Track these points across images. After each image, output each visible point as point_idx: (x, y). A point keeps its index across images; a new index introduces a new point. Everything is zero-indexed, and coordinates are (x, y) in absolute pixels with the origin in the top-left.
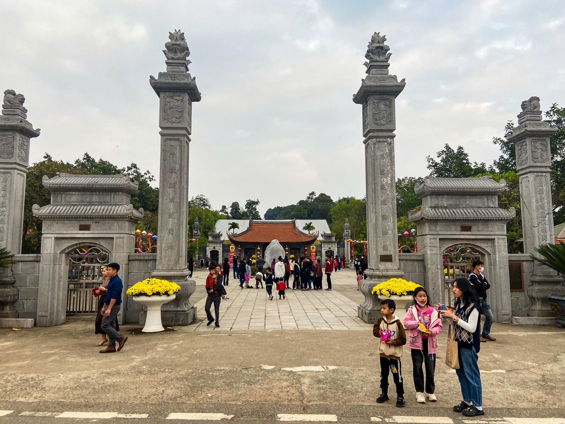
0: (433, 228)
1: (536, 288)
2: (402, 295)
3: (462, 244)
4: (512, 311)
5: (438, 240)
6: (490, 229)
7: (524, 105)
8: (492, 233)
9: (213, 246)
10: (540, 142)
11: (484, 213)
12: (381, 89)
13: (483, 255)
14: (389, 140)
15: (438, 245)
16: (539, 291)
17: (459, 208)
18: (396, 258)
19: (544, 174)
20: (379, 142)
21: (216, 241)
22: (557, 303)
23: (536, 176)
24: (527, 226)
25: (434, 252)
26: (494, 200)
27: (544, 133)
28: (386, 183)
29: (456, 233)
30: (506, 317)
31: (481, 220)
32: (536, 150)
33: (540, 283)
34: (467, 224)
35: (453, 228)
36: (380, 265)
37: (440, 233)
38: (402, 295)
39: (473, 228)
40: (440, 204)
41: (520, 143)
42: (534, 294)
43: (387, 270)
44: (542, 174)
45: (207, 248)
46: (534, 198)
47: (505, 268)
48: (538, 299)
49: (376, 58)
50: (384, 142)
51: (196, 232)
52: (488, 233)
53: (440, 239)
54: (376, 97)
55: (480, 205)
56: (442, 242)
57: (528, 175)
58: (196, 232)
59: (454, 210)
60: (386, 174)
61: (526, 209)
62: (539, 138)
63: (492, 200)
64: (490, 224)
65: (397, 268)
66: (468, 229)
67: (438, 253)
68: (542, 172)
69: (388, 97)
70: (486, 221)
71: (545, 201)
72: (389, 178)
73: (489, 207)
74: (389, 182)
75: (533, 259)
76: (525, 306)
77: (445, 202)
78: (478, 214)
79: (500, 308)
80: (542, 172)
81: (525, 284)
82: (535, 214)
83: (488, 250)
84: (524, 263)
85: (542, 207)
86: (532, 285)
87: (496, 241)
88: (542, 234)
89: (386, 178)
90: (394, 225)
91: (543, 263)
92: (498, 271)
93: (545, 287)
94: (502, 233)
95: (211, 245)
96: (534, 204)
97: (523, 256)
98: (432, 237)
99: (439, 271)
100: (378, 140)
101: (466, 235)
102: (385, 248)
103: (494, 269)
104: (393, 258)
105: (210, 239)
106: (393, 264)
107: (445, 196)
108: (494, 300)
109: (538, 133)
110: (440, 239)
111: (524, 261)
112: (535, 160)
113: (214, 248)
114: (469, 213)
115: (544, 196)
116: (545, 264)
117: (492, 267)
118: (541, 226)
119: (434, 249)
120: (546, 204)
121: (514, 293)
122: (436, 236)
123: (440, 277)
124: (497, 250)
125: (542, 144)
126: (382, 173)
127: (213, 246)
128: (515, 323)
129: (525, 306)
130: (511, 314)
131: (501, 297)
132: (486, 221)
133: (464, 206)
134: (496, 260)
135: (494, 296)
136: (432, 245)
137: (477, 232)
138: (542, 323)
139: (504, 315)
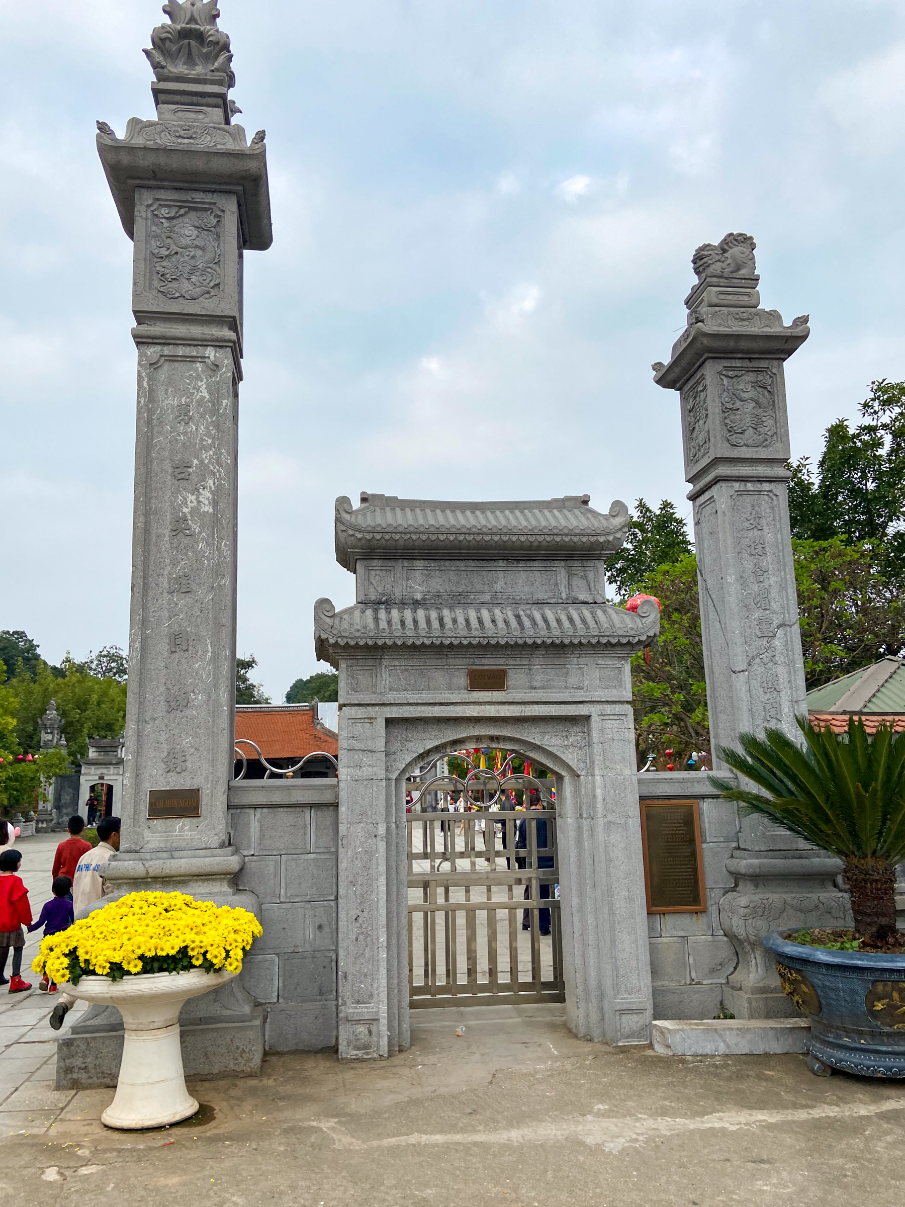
0: (363, 678)
1: (743, 901)
2: (117, 971)
3: (478, 739)
4: (656, 992)
6: (572, 680)
7: (701, 260)
8: (579, 696)
9: (99, 772)
10: (751, 377)
11: (553, 622)
12: (175, 163)
14: (210, 352)
15: (381, 743)
16: (754, 911)
17: (466, 605)
18: (214, 803)
19: (766, 486)
20: (173, 359)
21: (107, 759)
22: (799, 971)
23: (740, 493)
24: (716, 669)
25: (367, 772)
26: (591, 575)
27: (761, 345)
28: (195, 511)
29: (447, 692)
30: (632, 1022)
31: (535, 646)
32: (738, 404)
33: (758, 879)
34: (489, 663)
35: (440, 677)
36: (147, 835)
37: (390, 697)
38: (117, 971)
39: (516, 678)
40: (398, 593)
41: (693, 388)
42: (738, 926)
43: (172, 852)
44: (758, 486)
45: (83, 779)
46: (731, 570)
47: (626, 827)
48: (753, 945)
49: (180, 68)
50: (193, 359)
51: (50, 737)
53: (389, 722)
54: (162, 195)
55: (541, 596)
56: (399, 733)
57: (714, 491)
58: (50, 737)
59: (446, 612)
60: (194, 477)
61: (712, 615)
62: (746, 363)
63: (585, 577)
64: (573, 662)
65: (215, 841)
66: (493, 680)
67: (382, 774)
68: (760, 480)
69: (208, 198)
70: (558, 650)
71: (773, 580)
72: (207, 494)
73: (575, 602)
74: (207, 508)
75: (728, 793)
76: (713, 971)
77: (417, 581)
78: (527, 623)
79: (609, 992)
80: (760, 480)
81: (709, 883)
82: (735, 626)
83: (570, 757)
84: (706, 806)
85: (762, 601)
86: (733, 889)
87: (595, 722)
88: (764, 698)
89: (195, 491)
90: (217, 668)
91: (756, 804)
92: (601, 836)
93: (775, 897)
94: (613, 695)
95: (93, 770)
96: (732, 590)
97: (692, 781)
98: (360, 712)
99: (382, 846)
100: (167, 350)
101: (487, 704)
102: (174, 761)
103: (592, 829)
104: (204, 800)
105: (92, 753)
106: (202, 822)
107: (419, 564)
108: (592, 952)
109: (743, 345)
110: (389, 722)
111: (703, 797)
112: (734, 439)
113: (101, 778)
114: (498, 624)
115: (768, 561)
116: (757, 809)
117: (585, 823)
118: (757, 668)
119: (366, 759)
120: (774, 593)
121: (670, 920)
123: (383, 869)
124: (598, 758)
125: (756, 384)
126: (181, 472)
127: (99, 772)
128: (660, 1049)
129: (713, 971)
130: (649, 1006)
131: (613, 941)
132: (558, 650)
133: (487, 597)
134: (595, 796)
135: (591, 938)
136: (357, 745)
137: (529, 690)
138: (760, 1049)
139: (622, 1012)
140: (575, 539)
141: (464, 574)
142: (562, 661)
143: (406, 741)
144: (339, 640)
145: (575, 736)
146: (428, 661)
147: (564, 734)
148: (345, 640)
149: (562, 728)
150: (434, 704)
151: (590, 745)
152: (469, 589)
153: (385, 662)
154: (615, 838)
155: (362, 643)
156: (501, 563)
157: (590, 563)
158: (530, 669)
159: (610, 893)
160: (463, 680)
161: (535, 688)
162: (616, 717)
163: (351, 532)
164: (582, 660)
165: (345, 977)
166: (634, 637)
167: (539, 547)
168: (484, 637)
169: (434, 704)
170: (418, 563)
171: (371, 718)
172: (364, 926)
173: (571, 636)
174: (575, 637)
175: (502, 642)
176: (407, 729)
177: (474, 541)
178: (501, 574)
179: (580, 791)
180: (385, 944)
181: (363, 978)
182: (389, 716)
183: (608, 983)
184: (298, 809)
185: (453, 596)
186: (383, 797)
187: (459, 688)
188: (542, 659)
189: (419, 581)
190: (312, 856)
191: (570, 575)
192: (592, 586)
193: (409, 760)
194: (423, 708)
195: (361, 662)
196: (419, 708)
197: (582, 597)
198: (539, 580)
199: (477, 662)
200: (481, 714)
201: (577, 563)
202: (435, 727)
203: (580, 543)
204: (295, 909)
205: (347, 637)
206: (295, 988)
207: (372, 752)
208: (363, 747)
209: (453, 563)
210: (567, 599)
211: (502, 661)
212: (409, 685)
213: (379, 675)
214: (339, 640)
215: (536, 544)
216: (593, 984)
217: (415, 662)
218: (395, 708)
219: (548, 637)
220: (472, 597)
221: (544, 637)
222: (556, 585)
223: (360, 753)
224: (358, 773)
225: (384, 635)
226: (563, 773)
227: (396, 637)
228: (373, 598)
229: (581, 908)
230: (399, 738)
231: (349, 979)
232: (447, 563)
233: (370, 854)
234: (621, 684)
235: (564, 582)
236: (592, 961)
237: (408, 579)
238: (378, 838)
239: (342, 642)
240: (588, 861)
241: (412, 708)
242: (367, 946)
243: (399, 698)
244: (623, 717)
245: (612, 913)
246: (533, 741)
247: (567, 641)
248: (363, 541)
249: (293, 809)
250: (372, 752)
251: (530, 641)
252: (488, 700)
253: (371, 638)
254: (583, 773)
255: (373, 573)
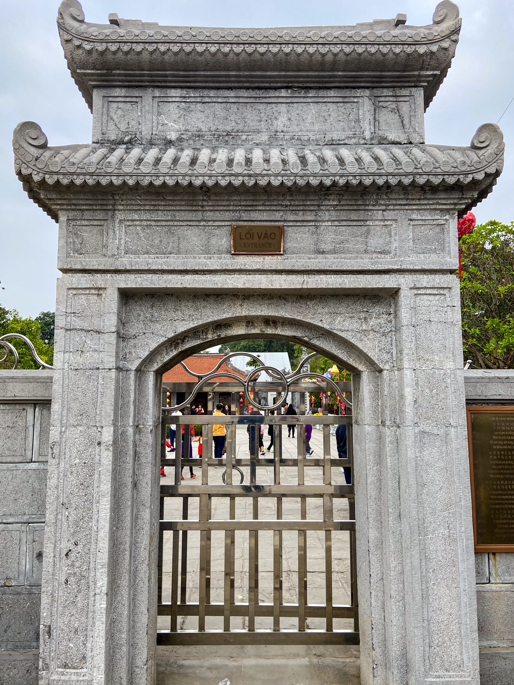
3: (249, 321)
5: (112, 299)
6: (374, 242)
13: (357, 374)
15: (111, 322)
25: (90, 359)
26: (405, 108)
29: (201, 253)
34: (262, 217)
35: (193, 237)
39: (297, 238)
40: (146, 131)
47: (446, 439)
52: (365, 263)
53: (127, 296)
56: (141, 311)
66: (264, 241)
67: (111, 361)
73: (383, 141)
83: (369, 346)
87: (405, 298)
92: (410, 452)
94: (432, 261)
98: (84, 281)
99: (106, 458)
101: (257, 272)
103: (397, 441)
108: (393, 606)
110: (127, 296)
117: (388, 433)
119: (90, 342)
122: (100, 280)
124: (408, 346)
131: (425, 597)
134: (402, 397)
135: (394, 588)
136: (78, 323)
140: (385, 50)
141: (234, 107)
142: (361, 215)
143: (151, 321)
144: (47, 176)
145: (377, 317)
146: (177, 214)
147: (363, 315)
148: (55, 177)
149: (359, 308)
150: (186, 272)
151: (397, 330)
152: (240, 127)
153: (120, 216)
154: (431, 453)
155: (78, 181)
156: (283, 93)
157: (405, 92)
158: (317, 227)
159: (422, 529)
160: (223, 240)
161: (323, 252)
162: (435, 292)
163: (77, 43)
164: (389, 215)
165: (49, 633)
166: (466, 174)
167: (334, 65)
168: (250, 176)
169: (186, 272)
170: (173, 92)
171: (99, 289)
172: (77, 564)
173: (373, 174)
174: (380, 175)
175: (276, 182)
176: (152, 306)
177: (243, 55)
178: (283, 108)
179: (383, 390)
180: (105, 589)
181: (72, 635)
182: (123, 285)
183: (416, 655)
184: (18, 407)
185: (219, 136)
186: (110, 393)
187: (220, 252)
188: (334, 213)
189: (175, 117)
190: (33, 466)
191: (376, 109)
192: (406, 121)
193: (153, 346)
194: (170, 277)
195: (87, 215)
196: (166, 277)
197: (392, 136)
198: (334, 115)
199: (245, 216)
200: (247, 286)
201: (386, 92)
202: (190, 304)
203: (391, 55)
204: (9, 531)
205: (57, 173)
206: (6, 631)
207: (99, 332)
208: (86, 325)
209: (221, 93)
210: (372, 139)
211: (278, 216)
212: (152, 246)
213: (111, 232)
214: (47, 176)
215: (329, 58)
216: (395, 650)
217: (160, 216)
218: (132, 277)
219: (341, 176)
220: (244, 137)
221: (334, 175)
222: (358, 121)
223: (83, 334)
224: (78, 360)
225: (109, 170)
226: (361, 367)
227: (126, 175)
228: (113, 137)
229: (381, 544)
230: (141, 318)
231: (54, 634)
232: (212, 93)
233: (91, 466)
234: (443, 248)
235: (369, 116)
236: (394, 619)
237: (159, 114)
238: (103, 447)
239: (51, 180)
240: (391, 484)
241: (155, 277)
242: (79, 591)
243: (137, 263)
244: (446, 292)
245: (424, 556)
246: (320, 324)
247: (367, 181)
248: (95, 55)
249: (12, 407)
250: (99, 332)
251: (314, 182)
252: (258, 267)
253: (92, 174)
254: (387, 367)
255: (114, 105)
